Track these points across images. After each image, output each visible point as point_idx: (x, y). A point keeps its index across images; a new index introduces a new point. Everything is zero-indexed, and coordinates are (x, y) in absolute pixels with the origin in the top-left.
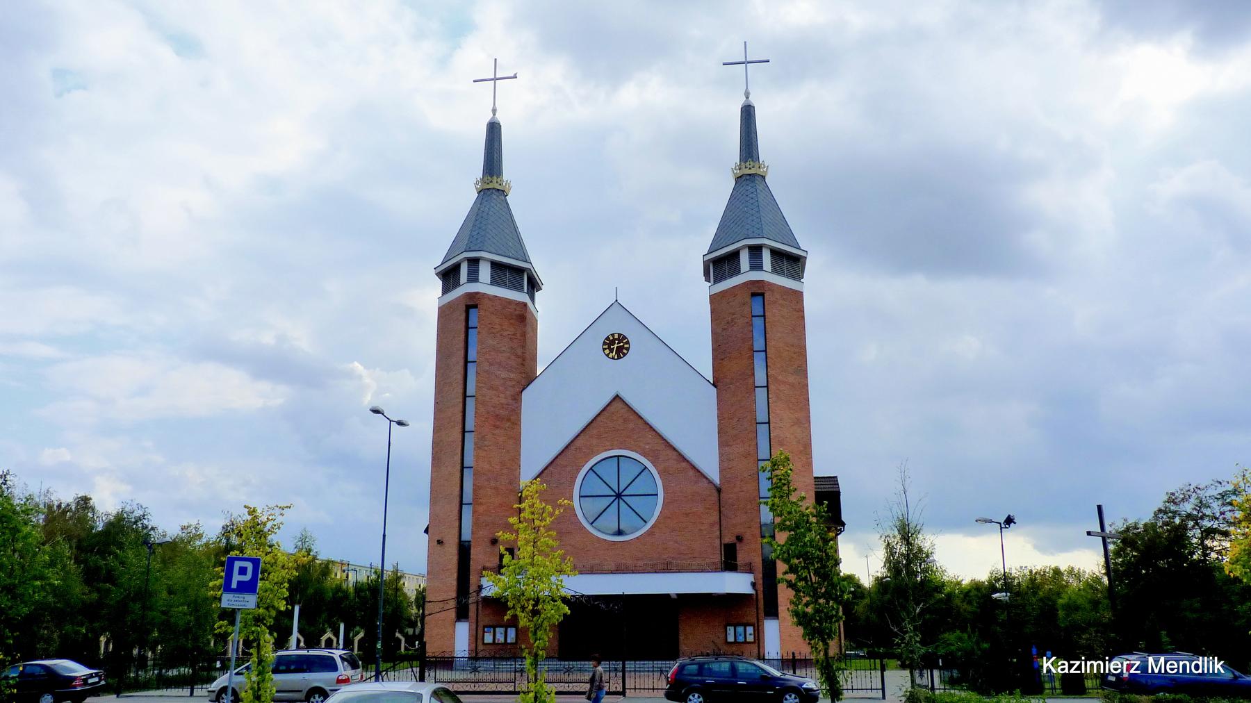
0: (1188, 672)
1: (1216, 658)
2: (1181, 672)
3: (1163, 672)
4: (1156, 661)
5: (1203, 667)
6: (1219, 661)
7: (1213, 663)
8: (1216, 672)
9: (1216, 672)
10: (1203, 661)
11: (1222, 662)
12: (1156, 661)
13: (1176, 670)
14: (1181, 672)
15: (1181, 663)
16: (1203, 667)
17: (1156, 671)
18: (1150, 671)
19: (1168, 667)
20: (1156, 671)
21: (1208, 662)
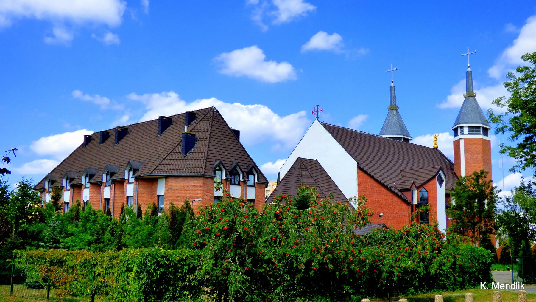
0: (509, 289)
1: (521, 283)
2: (506, 289)
3: (498, 289)
4: (496, 285)
5: (516, 286)
6: (522, 284)
7: (520, 286)
8: (521, 289)
9: (521, 289)
10: (516, 284)
11: (524, 285)
12: (496, 285)
13: (504, 288)
14: (506, 289)
15: (506, 285)
16: (516, 288)
17: (496, 288)
18: (493, 289)
19: (501, 287)
20: (496, 288)
21: (518, 284)
